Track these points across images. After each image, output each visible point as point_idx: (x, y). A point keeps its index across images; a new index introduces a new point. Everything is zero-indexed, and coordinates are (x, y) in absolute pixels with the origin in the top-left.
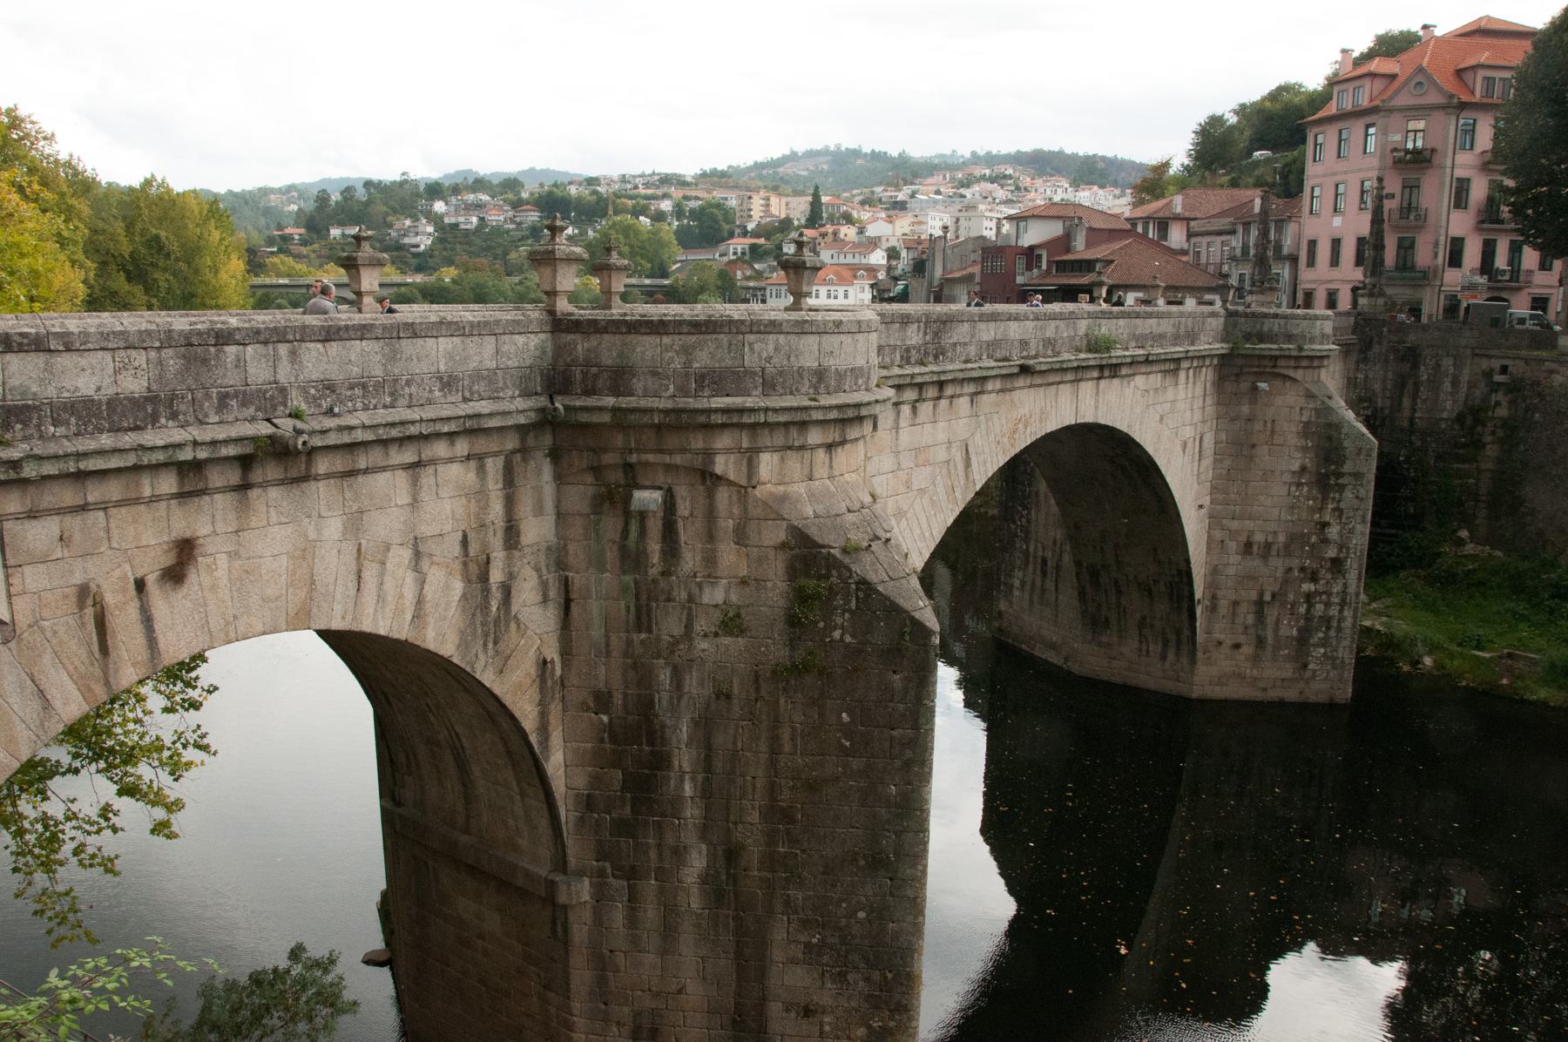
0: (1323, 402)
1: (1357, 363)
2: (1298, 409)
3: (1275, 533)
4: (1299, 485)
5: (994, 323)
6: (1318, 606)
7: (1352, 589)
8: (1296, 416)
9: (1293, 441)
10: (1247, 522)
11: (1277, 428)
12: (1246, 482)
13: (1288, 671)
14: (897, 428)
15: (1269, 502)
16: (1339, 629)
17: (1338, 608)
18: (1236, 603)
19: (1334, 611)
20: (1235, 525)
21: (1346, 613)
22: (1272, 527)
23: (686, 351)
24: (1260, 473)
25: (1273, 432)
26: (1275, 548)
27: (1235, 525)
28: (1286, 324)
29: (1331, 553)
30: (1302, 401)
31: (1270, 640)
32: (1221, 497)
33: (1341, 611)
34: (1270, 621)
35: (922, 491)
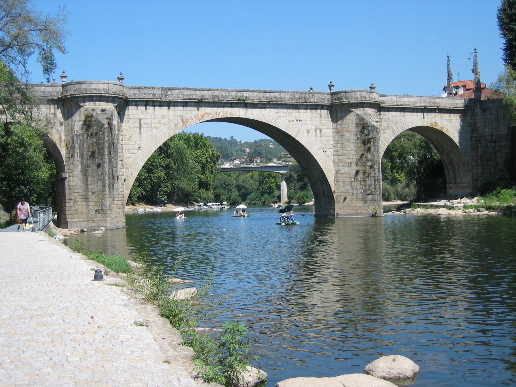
0: (361, 117)
1: (470, 117)
2: (354, 119)
3: (353, 159)
4: (357, 143)
5: (189, 91)
6: (368, 181)
7: (377, 175)
8: (354, 121)
9: (354, 129)
10: (344, 156)
11: (349, 126)
12: (342, 144)
13: (361, 204)
14: (154, 111)
15: (349, 149)
16: (375, 189)
17: (374, 181)
18: (344, 182)
19: (373, 183)
20: (341, 157)
21: (376, 183)
22: (352, 157)
23: (74, 87)
24: (346, 140)
25: (348, 127)
26: (353, 163)
27: (341, 157)
28: (346, 94)
29: (369, 164)
30: (355, 117)
31: (355, 194)
32: (336, 149)
33: (375, 182)
34: (354, 187)
35: (164, 124)
